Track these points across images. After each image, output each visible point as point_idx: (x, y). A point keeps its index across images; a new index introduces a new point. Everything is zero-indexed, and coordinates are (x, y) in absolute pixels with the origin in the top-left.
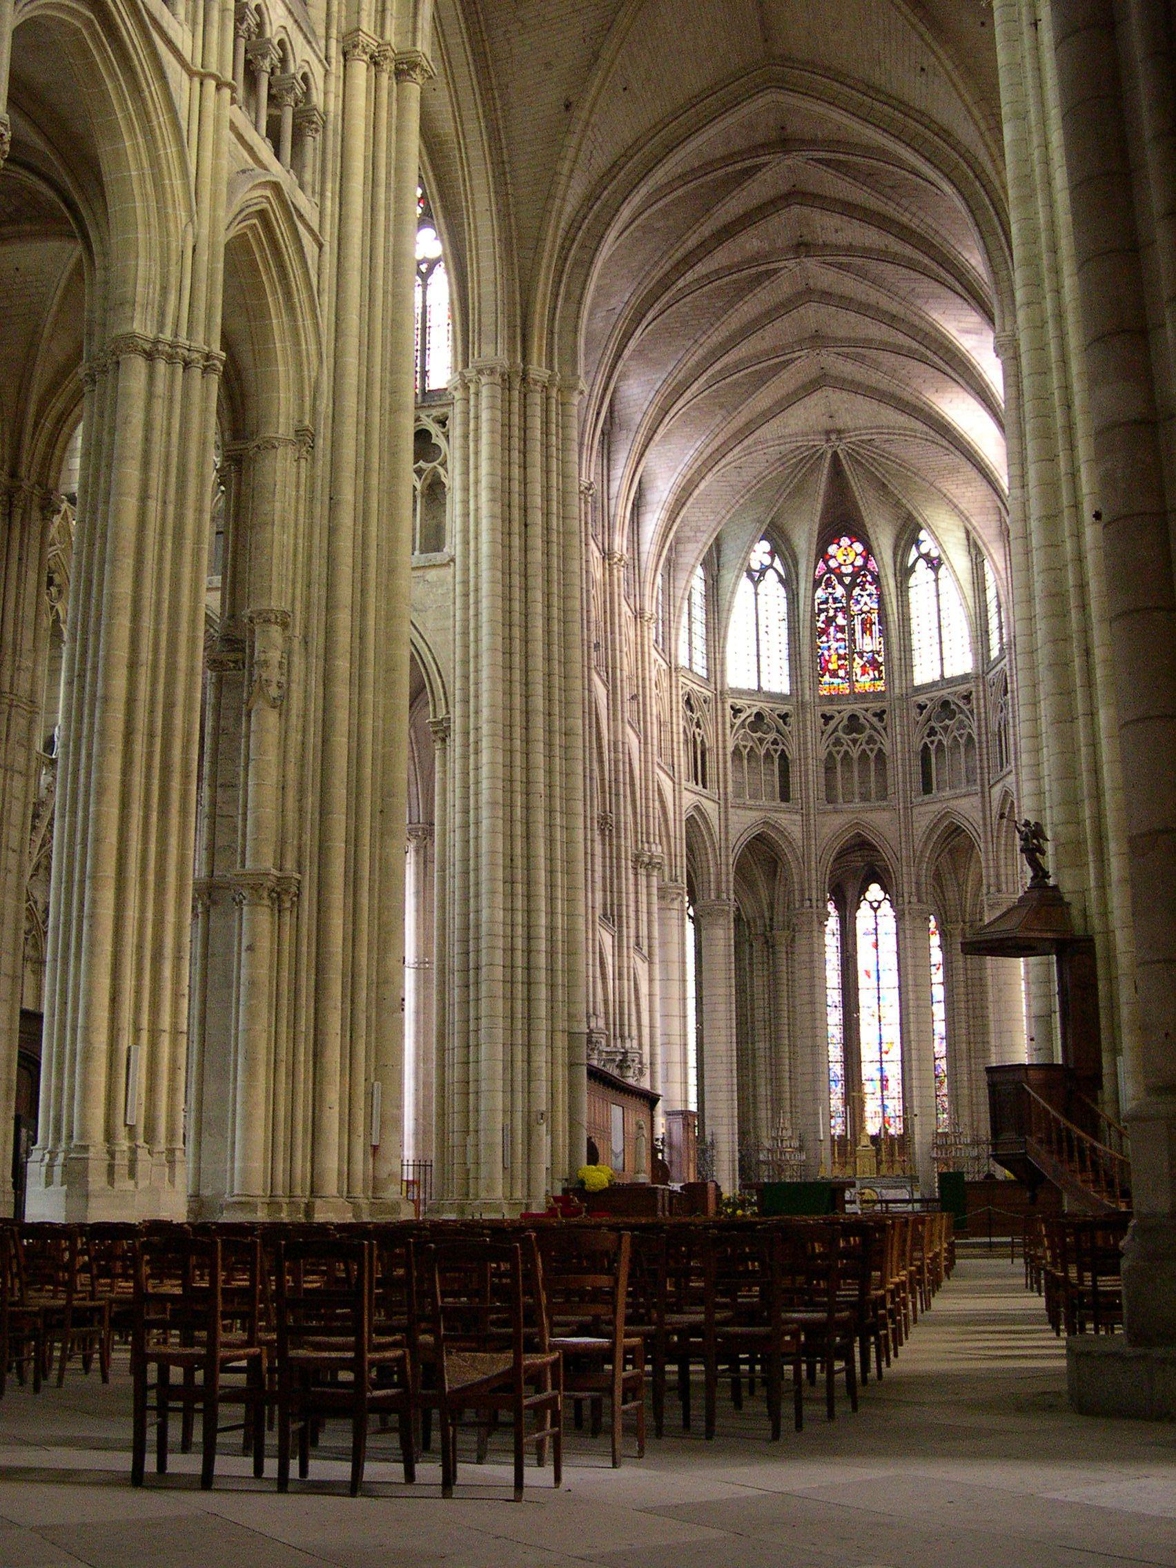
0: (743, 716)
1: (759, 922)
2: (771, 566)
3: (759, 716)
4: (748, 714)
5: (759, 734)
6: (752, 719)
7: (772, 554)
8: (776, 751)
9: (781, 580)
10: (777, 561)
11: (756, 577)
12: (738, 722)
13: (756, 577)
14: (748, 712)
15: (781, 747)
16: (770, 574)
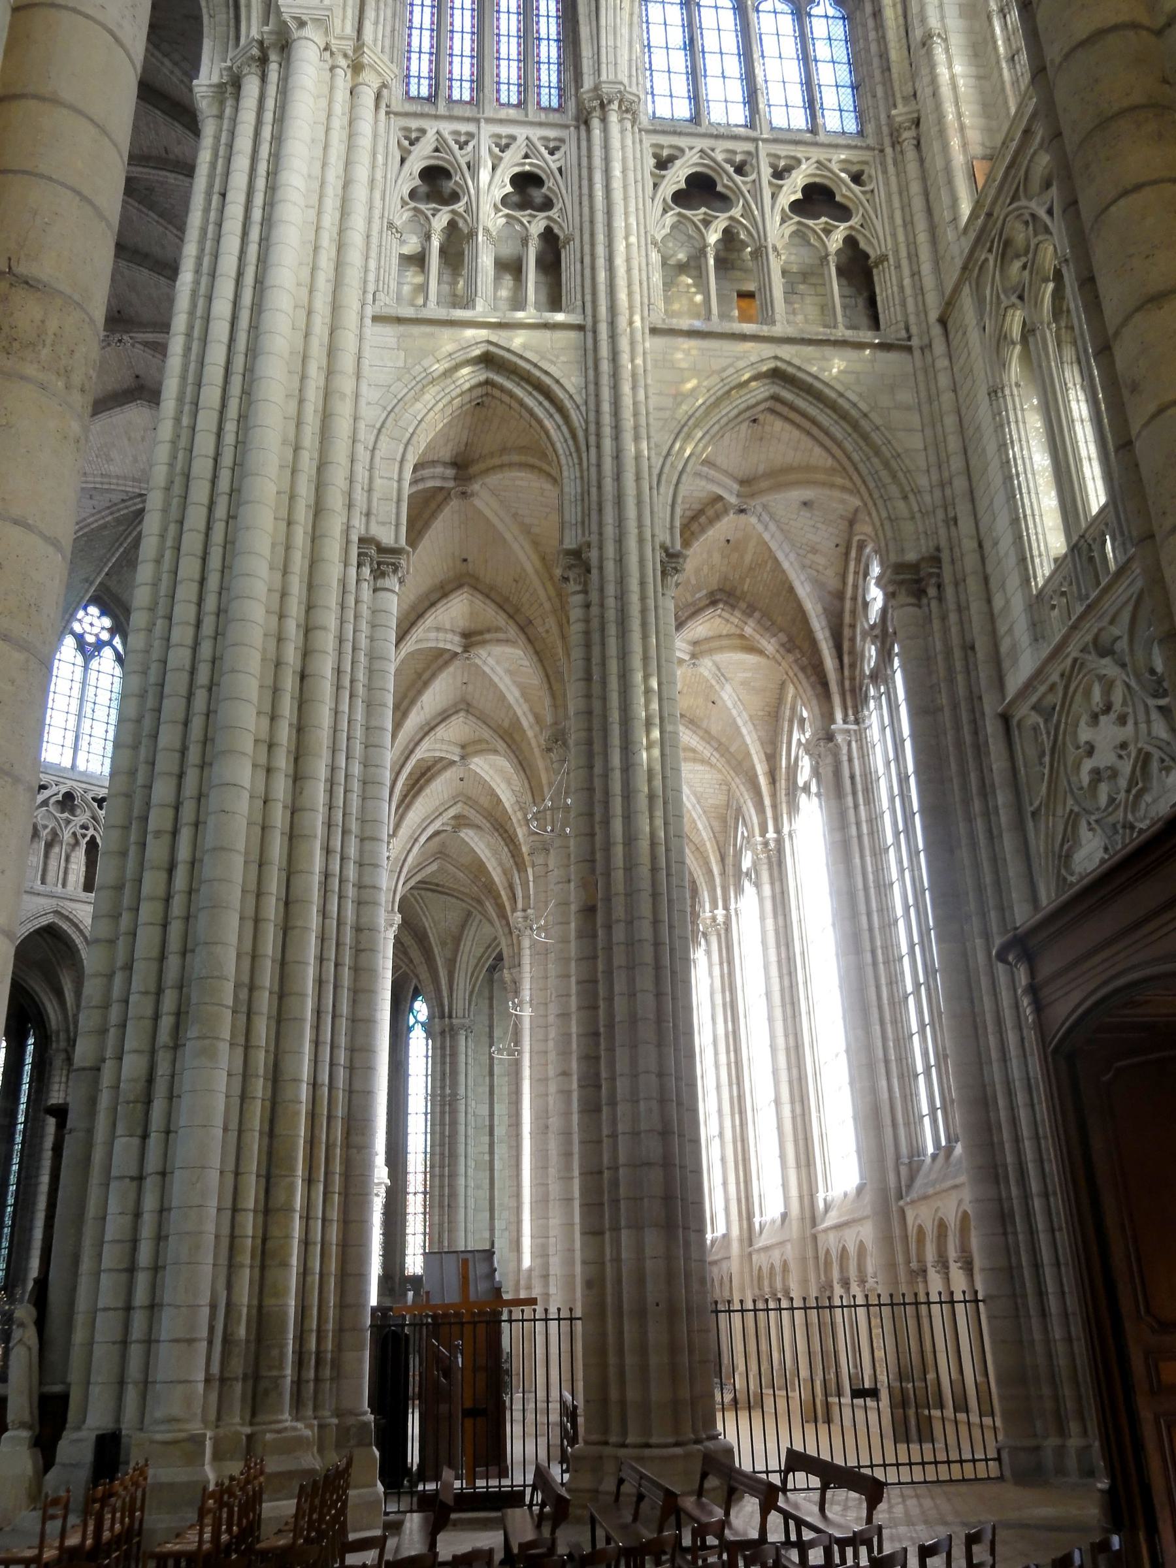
0: (46, 794)
1: (62, 1036)
2: (109, 643)
3: (68, 798)
4: (57, 791)
5: (66, 815)
6: (60, 797)
7: (113, 631)
8: (84, 836)
9: (119, 659)
10: (117, 641)
11: (88, 651)
12: (40, 798)
13: (88, 651)
14: (54, 789)
15: (91, 832)
16: (107, 652)
